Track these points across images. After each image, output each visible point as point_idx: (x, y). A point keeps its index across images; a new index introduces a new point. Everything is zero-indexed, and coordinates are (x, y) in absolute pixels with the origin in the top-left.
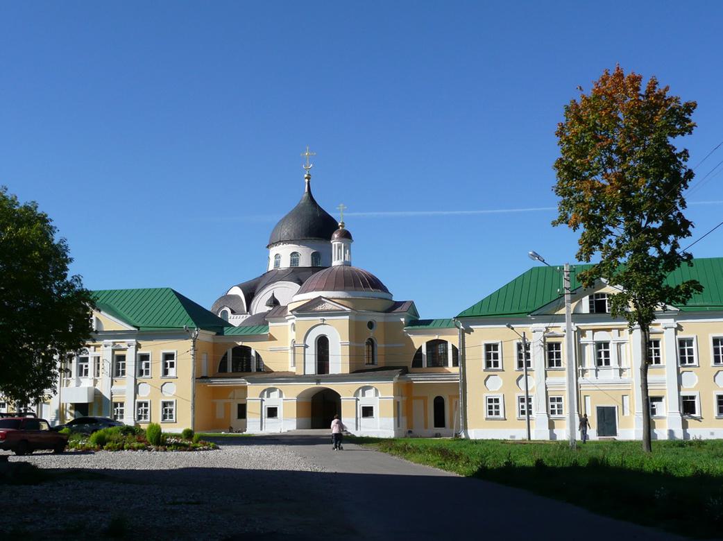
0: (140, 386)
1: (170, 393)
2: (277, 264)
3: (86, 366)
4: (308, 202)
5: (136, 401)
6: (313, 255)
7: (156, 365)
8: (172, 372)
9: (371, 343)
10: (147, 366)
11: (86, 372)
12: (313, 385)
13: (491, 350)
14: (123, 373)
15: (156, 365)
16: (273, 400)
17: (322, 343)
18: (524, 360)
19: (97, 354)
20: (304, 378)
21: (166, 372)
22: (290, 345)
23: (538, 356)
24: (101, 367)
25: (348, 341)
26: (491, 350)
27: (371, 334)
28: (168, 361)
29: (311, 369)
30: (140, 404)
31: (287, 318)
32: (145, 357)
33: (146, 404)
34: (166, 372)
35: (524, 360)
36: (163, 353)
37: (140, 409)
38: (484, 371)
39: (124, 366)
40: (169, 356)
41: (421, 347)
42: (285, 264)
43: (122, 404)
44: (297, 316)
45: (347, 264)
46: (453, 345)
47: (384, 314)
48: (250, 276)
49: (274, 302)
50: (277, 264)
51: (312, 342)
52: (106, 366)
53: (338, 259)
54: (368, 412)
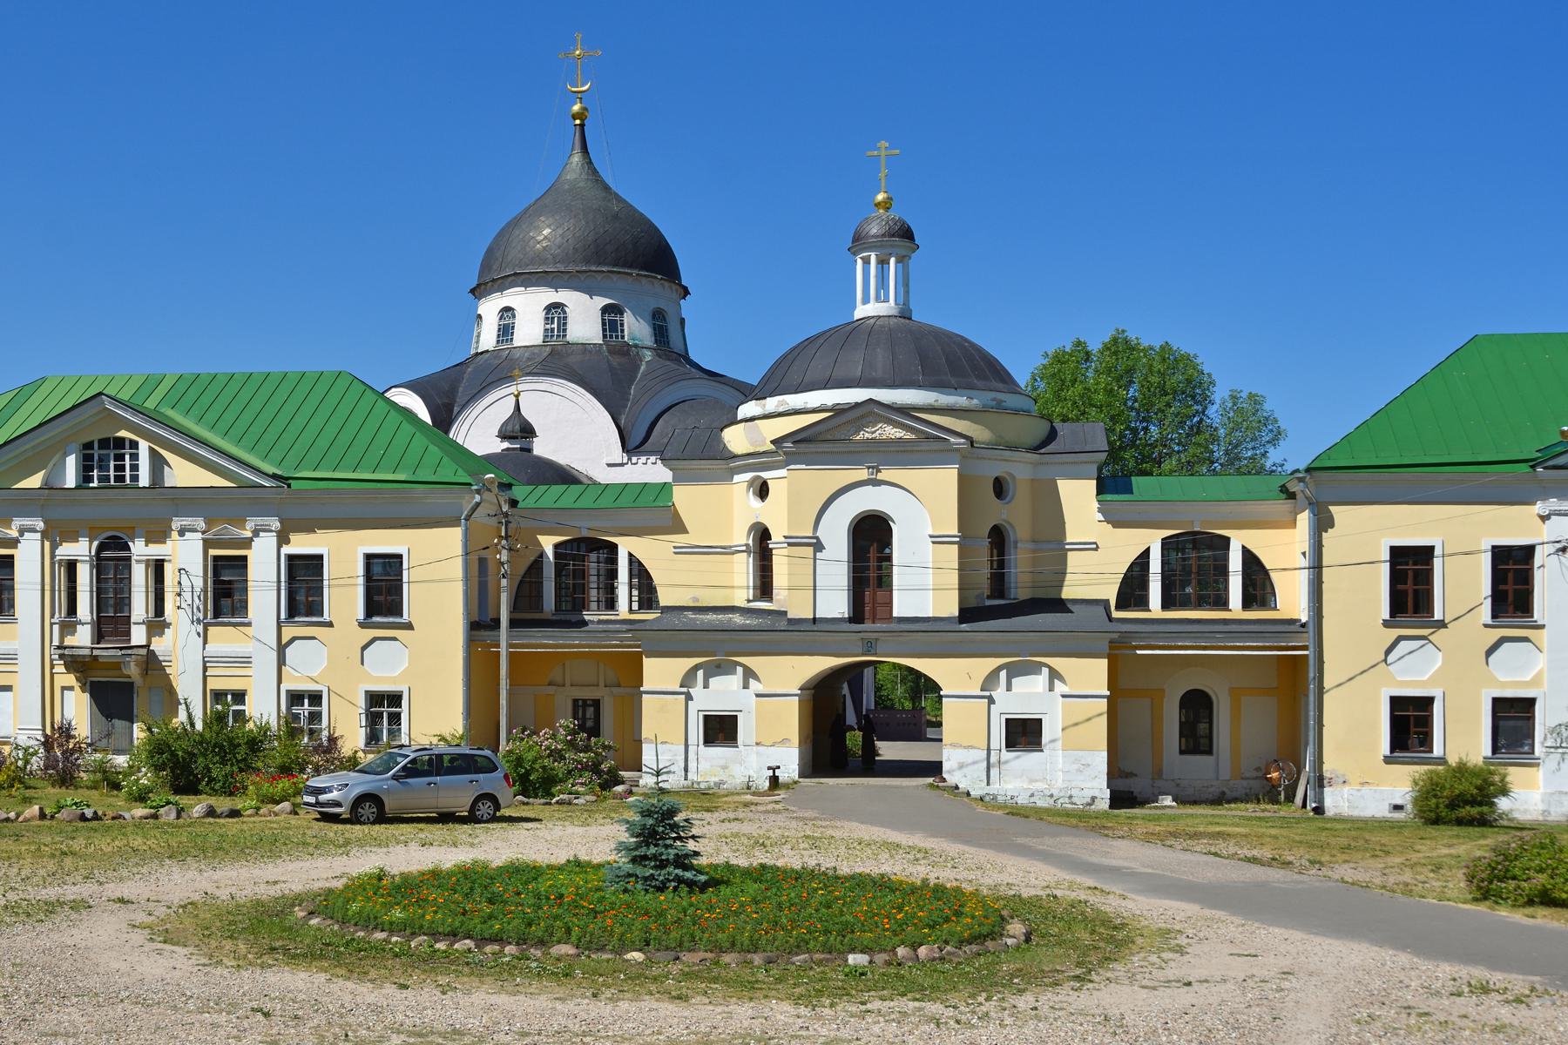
0: (288, 651)
2: (506, 331)
4: (584, 176)
5: (284, 688)
6: (606, 310)
9: (998, 537)
22: (741, 536)
25: (955, 532)
27: (997, 512)
29: (835, 604)
30: (296, 698)
33: (316, 698)
37: (296, 710)
38: (1386, 624)
41: (1148, 550)
42: (529, 332)
43: (240, 696)
45: (905, 314)
48: (433, 364)
49: (519, 430)
50: (506, 331)
53: (878, 299)
54: (1024, 734)
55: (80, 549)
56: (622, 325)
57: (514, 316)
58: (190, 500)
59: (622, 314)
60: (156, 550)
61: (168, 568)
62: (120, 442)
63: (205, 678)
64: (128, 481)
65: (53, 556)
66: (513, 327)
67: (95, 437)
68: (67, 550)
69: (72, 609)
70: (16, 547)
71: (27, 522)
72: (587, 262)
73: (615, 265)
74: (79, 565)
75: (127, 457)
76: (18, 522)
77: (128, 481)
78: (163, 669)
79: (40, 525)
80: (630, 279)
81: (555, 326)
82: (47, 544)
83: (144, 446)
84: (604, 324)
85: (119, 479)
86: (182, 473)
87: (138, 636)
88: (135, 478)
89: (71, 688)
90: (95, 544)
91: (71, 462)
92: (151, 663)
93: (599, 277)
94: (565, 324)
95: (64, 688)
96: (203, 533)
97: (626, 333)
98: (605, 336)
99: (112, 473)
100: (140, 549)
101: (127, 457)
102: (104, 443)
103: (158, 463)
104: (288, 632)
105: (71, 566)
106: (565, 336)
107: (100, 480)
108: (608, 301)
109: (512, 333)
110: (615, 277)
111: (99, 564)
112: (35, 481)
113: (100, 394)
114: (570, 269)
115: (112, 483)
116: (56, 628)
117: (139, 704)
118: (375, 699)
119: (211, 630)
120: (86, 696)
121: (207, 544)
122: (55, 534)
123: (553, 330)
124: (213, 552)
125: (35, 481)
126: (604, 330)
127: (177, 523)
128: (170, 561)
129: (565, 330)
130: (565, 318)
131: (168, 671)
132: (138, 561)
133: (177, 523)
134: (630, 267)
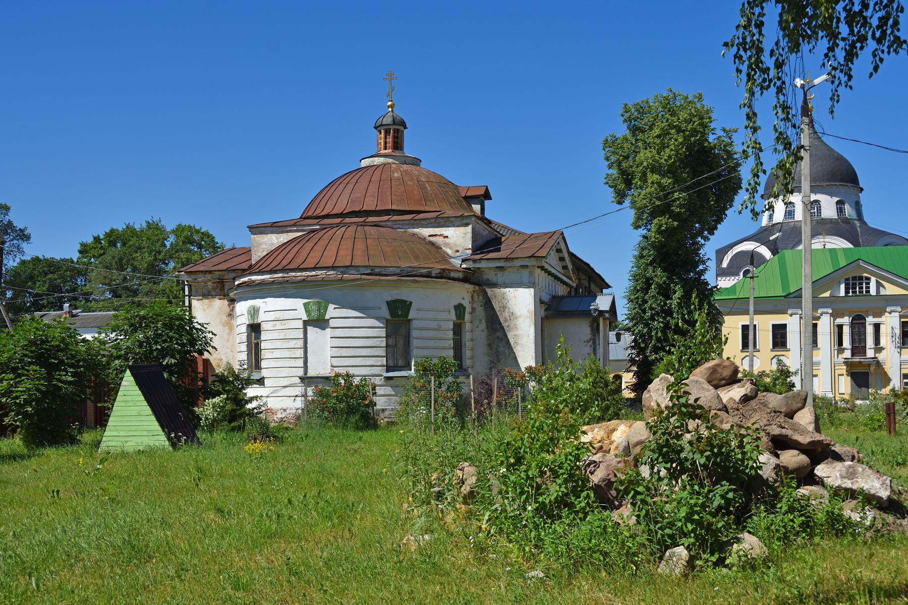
6: (837, 203)
55: (846, 320)
56: (845, 209)
57: (794, 206)
58: (893, 300)
59: (844, 204)
60: (877, 320)
61: (882, 328)
62: (861, 278)
63: (901, 369)
64: (864, 293)
65: (834, 323)
66: (794, 212)
67: (850, 276)
68: (839, 321)
69: (840, 343)
70: (819, 320)
71: (825, 310)
72: (829, 180)
73: (841, 182)
74: (844, 327)
75: (864, 284)
76: (820, 311)
77: (864, 293)
78: (882, 366)
79: (830, 311)
80: (847, 188)
81: (816, 210)
82: (832, 319)
83: (873, 280)
84: (837, 209)
85: (861, 292)
86: (890, 290)
87: (870, 353)
88: (868, 292)
89: (842, 375)
90: (851, 318)
91: (843, 286)
92: (878, 364)
93: (834, 187)
94: (820, 210)
95: (839, 375)
96: (899, 312)
97: (846, 213)
98: (838, 215)
99: (864, 290)
100: (870, 320)
101: (864, 284)
102: (854, 278)
103: (879, 285)
105: (840, 327)
106: (821, 215)
107: (853, 292)
108: (838, 199)
109: (794, 215)
110: (841, 187)
111: (852, 325)
112: (827, 294)
113: (859, 259)
114: (821, 184)
115: (858, 293)
116: (836, 351)
117: (871, 380)
119: (903, 350)
120: (849, 378)
121: (901, 317)
122: (834, 315)
123: (815, 212)
124: (902, 320)
125: (827, 294)
126: (838, 212)
127: (888, 309)
128: (884, 324)
129: (820, 213)
130: (820, 207)
131: (884, 367)
132: (870, 324)
133: (888, 309)
134: (846, 182)
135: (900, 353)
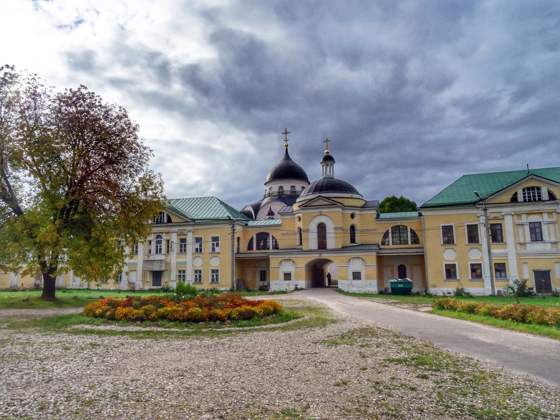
1: (215, 263)
3: (160, 246)
7: (208, 246)
8: (217, 250)
10: (201, 245)
11: (160, 249)
12: (316, 256)
13: (448, 231)
14: (185, 251)
15: (208, 246)
16: (287, 267)
17: (322, 228)
18: (473, 237)
19: (167, 238)
20: (311, 251)
21: (213, 249)
23: (483, 234)
24: (170, 246)
26: (448, 231)
28: (215, 243)
30: (196, 272)
31: (294, 213)
32: (198, 240)
34: (213, 249)
35: (473, 237)
36: (211, 237)
39: (185, 246)
40: (215, 239)
43: (184, 272)
44: (302, 209)
46: (411, 229)
47: (361, 209)
51: (313, 227)
52: (176, 247)
54: (357, 276)
104: (195, 256)
118: (213, 271)
135: (177, 258)
